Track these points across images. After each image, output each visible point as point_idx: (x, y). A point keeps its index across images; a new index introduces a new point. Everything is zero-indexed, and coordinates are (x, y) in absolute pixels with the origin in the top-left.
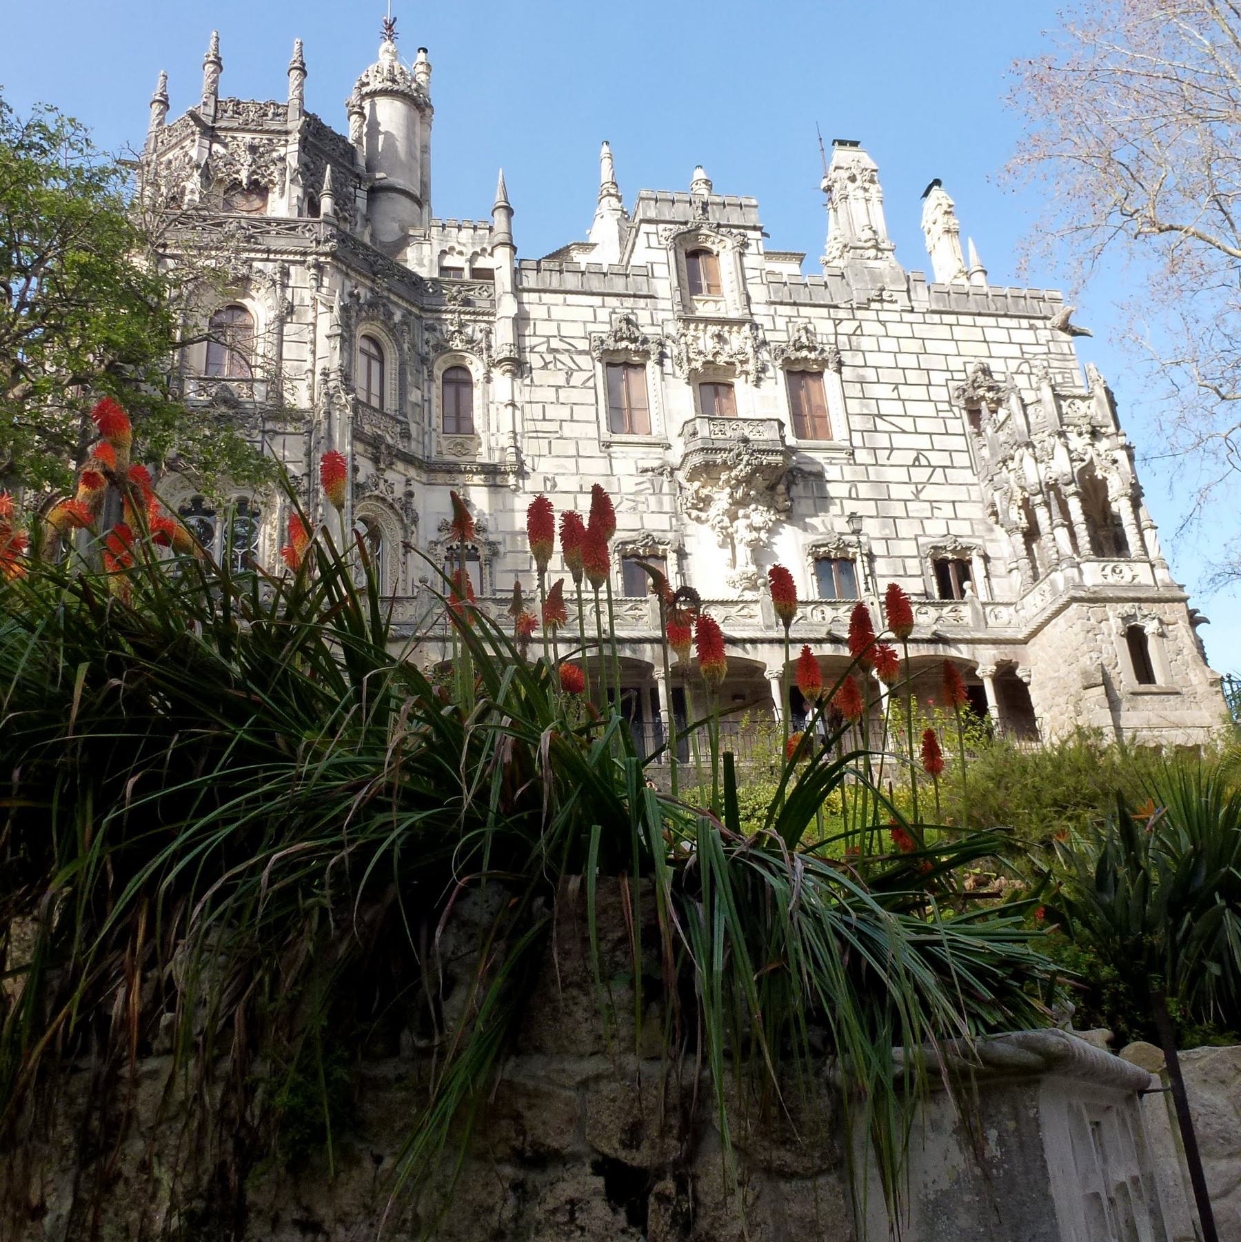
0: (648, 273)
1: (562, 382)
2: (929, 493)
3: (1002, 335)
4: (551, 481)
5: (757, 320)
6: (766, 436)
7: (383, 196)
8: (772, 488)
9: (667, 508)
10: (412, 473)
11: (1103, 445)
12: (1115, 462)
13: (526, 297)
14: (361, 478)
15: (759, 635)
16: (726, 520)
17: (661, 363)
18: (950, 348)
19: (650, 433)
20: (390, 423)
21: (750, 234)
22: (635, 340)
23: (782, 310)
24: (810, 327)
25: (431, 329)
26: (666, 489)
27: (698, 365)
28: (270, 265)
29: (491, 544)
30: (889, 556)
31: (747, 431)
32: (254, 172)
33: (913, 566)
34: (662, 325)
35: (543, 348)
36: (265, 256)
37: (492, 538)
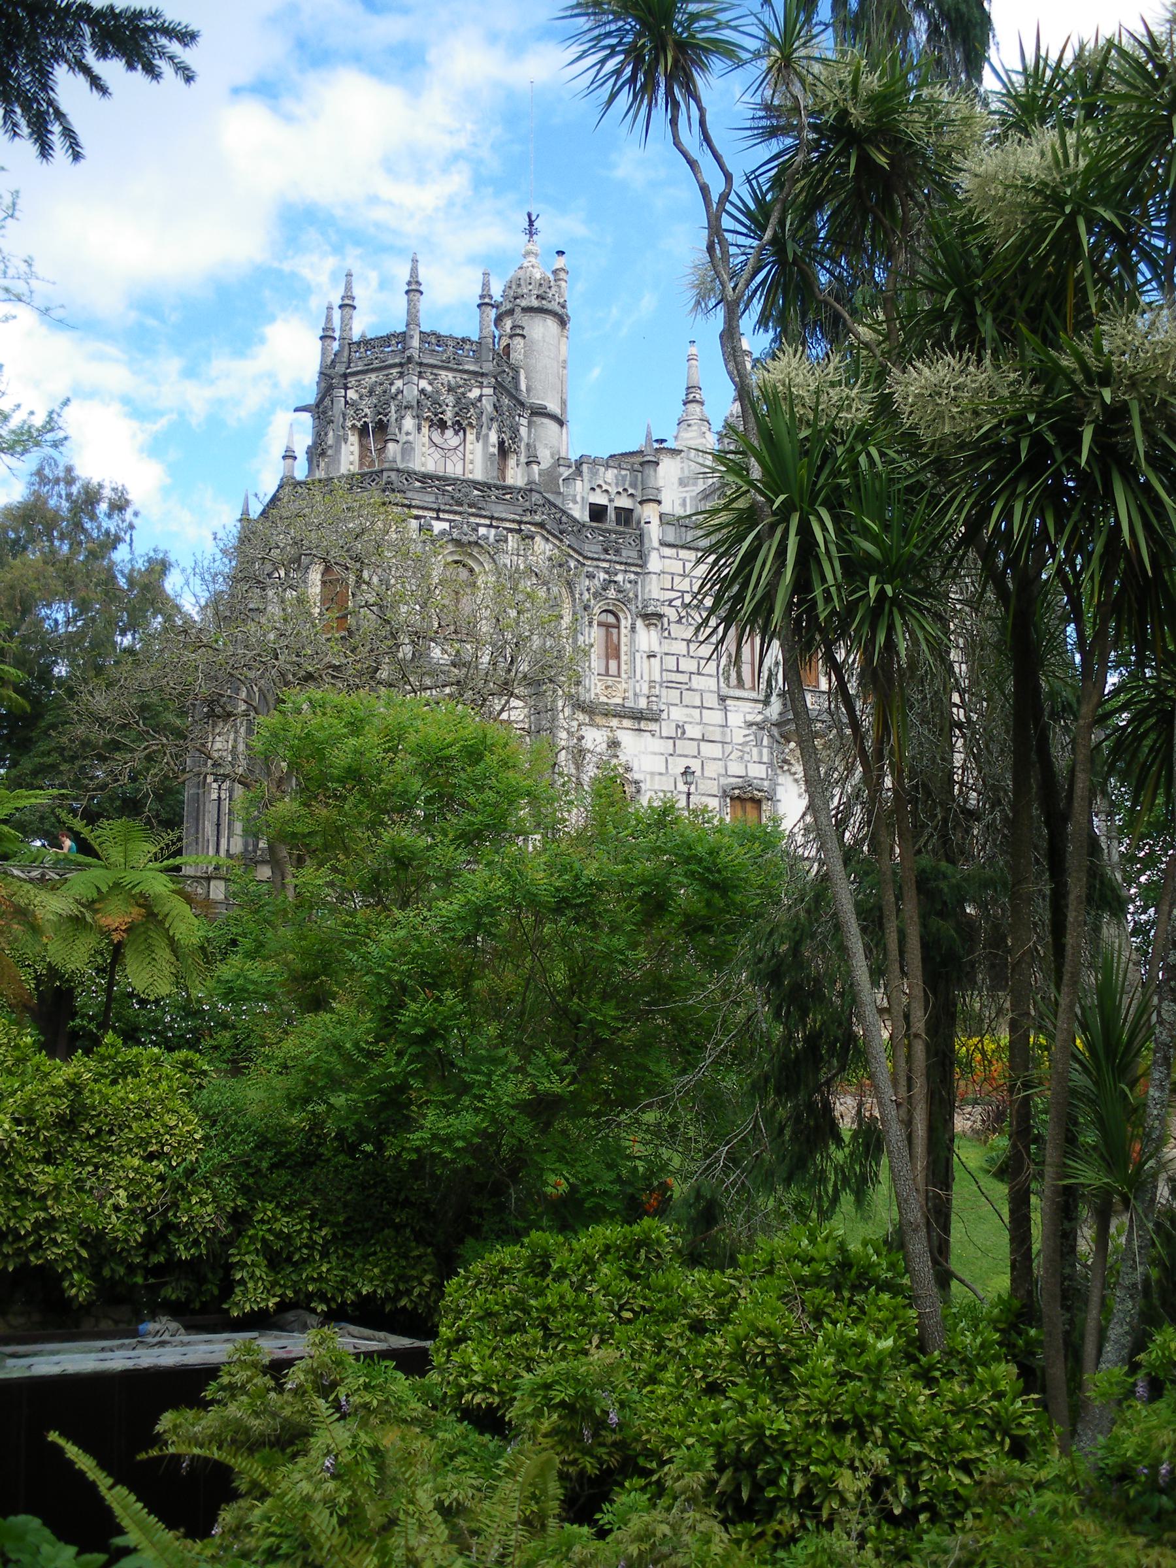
9: (765, 759)
25: (591, 576)
28: (493, 531)
32: (457, 414)
35: (678, 603)
36: (488, 522)
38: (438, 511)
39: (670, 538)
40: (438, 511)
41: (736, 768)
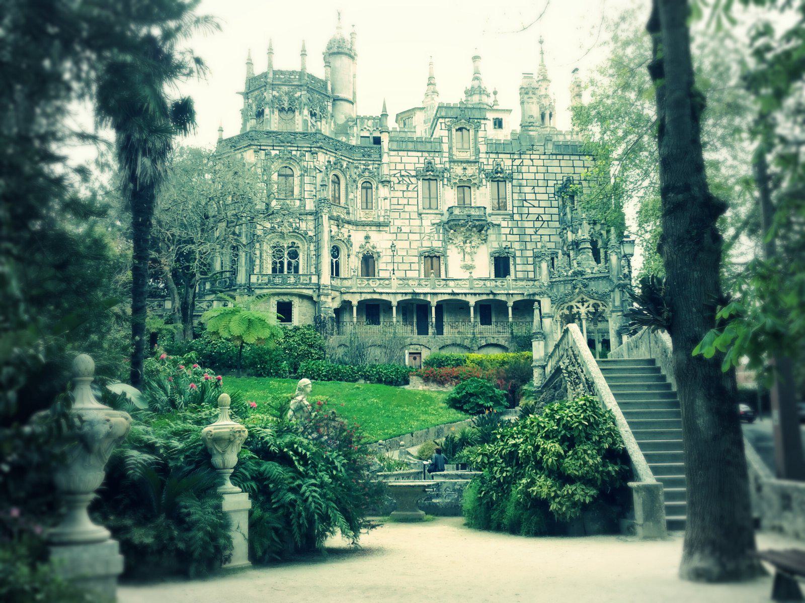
0: (441, 142)
1: (405, 189)
2: (541, 232)
3: (580, 163)
4: (400, 229)
5: (481, 160)
6: (478, 214)
7: (338, 102)
8: (480, 231)
9: (441, 238)
10: (350, 227)
11: (598, 227)
12: (601, 234)
13: (392, 153)
14: (333, 233)
15: (467, 291)
16: (462, 244)
17: (442, 180)
18: (558, 170)
19: (437, 208)
20: (342, 209)
21: (482, 121)
22: (433, 171)
23: (491, 155)
24: (502, 163)
25: (357, 168)
26: (441, 231)
27: (457, 181)
28: (299, 152)
29: (378, 253)
30: (522, 257)
31: (473, 212)
33: (531, 260)
34: (444, 164)
35: (398, 175)
36: (296, 149)
37: (378, 250)
38: (273, 146)
39: (395, 147)
40: (273, 146)
41: (426, 244)
